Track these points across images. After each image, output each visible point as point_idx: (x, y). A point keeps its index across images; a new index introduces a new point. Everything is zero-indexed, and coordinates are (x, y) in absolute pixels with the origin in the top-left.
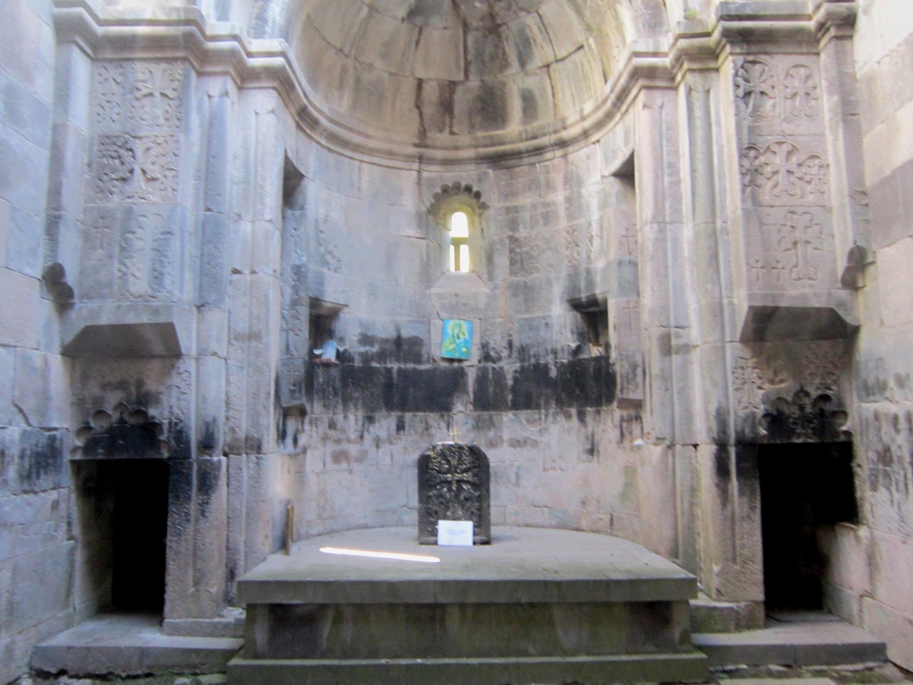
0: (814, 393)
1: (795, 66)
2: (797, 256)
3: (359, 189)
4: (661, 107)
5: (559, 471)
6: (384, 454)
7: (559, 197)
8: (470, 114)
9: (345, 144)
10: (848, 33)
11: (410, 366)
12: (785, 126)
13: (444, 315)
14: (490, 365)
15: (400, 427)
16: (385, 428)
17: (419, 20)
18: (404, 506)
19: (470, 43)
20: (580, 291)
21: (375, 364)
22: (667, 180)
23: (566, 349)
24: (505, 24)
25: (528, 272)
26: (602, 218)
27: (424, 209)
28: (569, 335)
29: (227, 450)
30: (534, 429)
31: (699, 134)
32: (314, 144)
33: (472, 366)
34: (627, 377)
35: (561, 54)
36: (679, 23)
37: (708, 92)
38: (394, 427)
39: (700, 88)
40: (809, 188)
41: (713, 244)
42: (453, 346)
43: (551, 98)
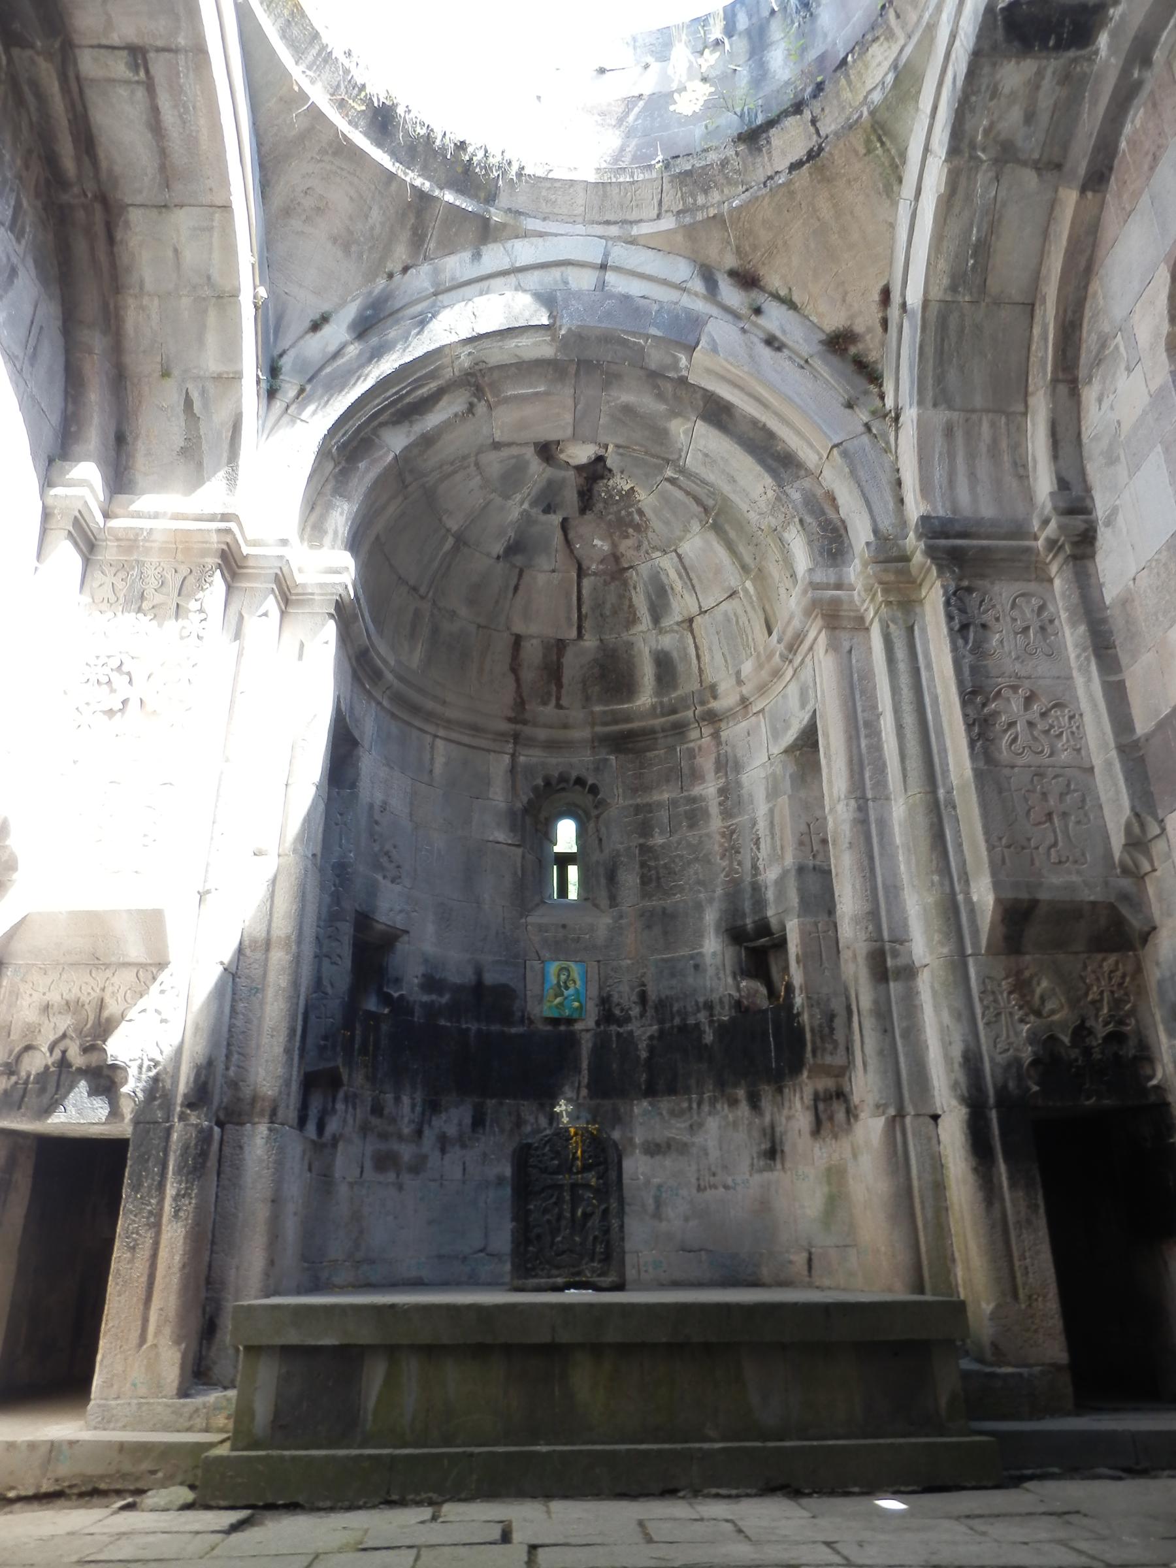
0: (1101, 1031)
2: (1055, 832)
3: (431, 771)
4: (850, 651)
5: (722, 1190)
6: (452, 1165)
7: (709, 789)
8: (584, 682)
9: (415, 709)
11: (495, 1028)
13: (546, 954)
14: (614, 1028)
15: (478, 1122)
16: (455, 1121)
17: (519, 560)
18: (481, 1251)
19: (584, 592)
20: (744, 916)
21: (442, 1022)
22: (864, 743)
23: (726, 1000)
26: (771, 811)
27: (519, 805)
28: (730, 980)
29: (222, 1116)
30: (683, 1126)
31: (905, 680)
32: (374, 704)
33: (587, 1031)
34: (821, 1031)
36: (868, 544)
37: (910, 630)
38: (468, 1120)
41: (935, 820)
42: (558, 1000)
43: (694, 661)
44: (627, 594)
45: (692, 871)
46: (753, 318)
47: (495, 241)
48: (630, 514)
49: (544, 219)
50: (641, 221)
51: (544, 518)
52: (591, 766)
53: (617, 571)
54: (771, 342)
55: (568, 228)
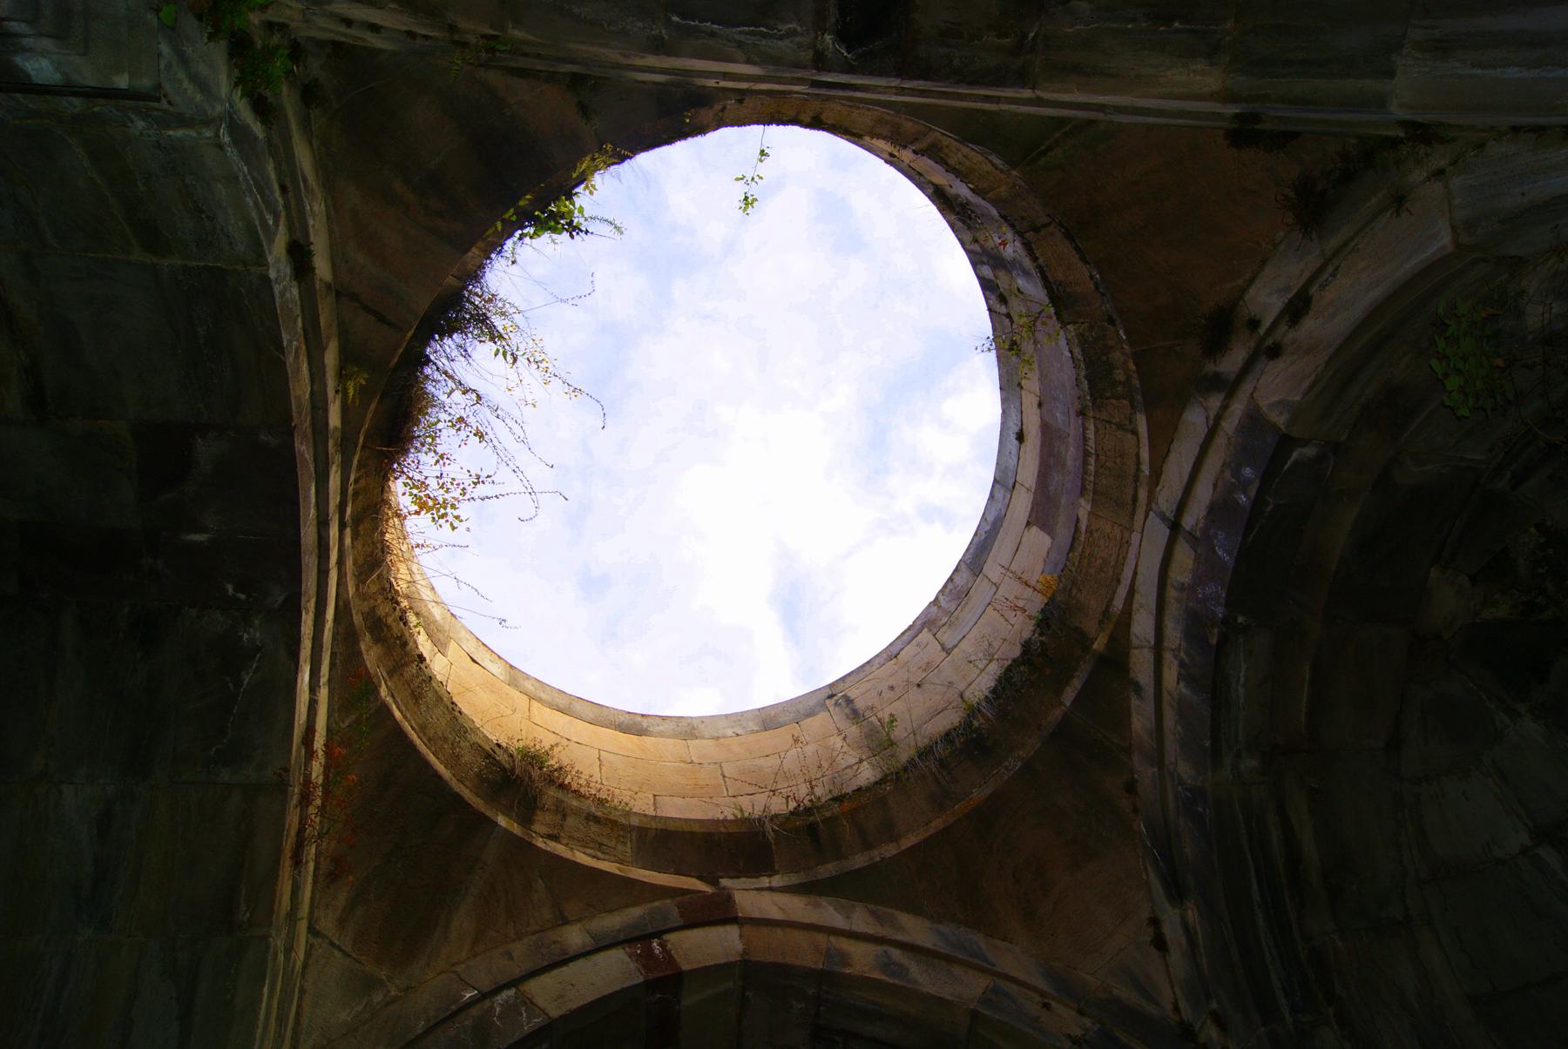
46: (1262, 331)
47: (1127, 655)
49: (1119, 581)
50: (1138, 455)
54: (1297, 308)
55: (1132, 551)
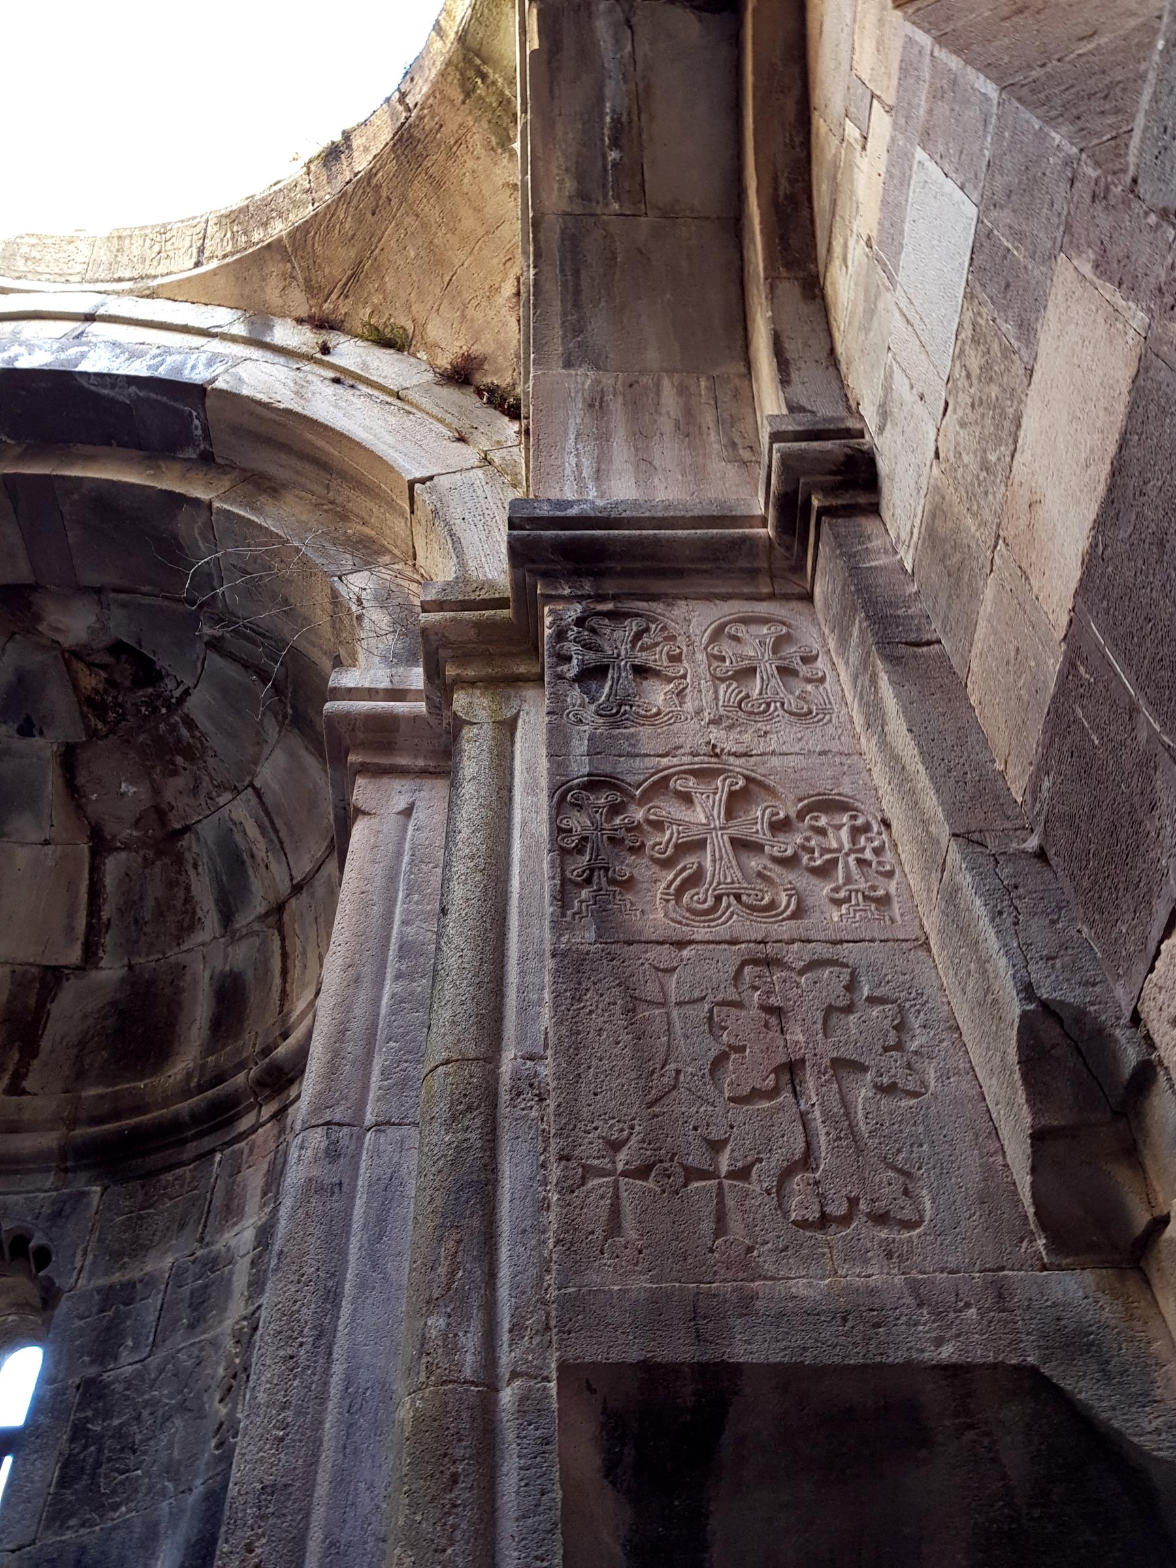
1: (745, 621)
4: (408, 812)
8: (82, 1044)
10: (862, 499)
12: (716, 734)
19: (110, 881)
24: (187, 829)
25: (101, 1508)
35: (302, 867)
39: (482, 715)
40: (826, 889)
43: (277, 980)
44: (182, 879)
45: (164, 1439)
48: (173, 728)
51: (20, 744)
52: (46, 1210)
53: (165, 839)
